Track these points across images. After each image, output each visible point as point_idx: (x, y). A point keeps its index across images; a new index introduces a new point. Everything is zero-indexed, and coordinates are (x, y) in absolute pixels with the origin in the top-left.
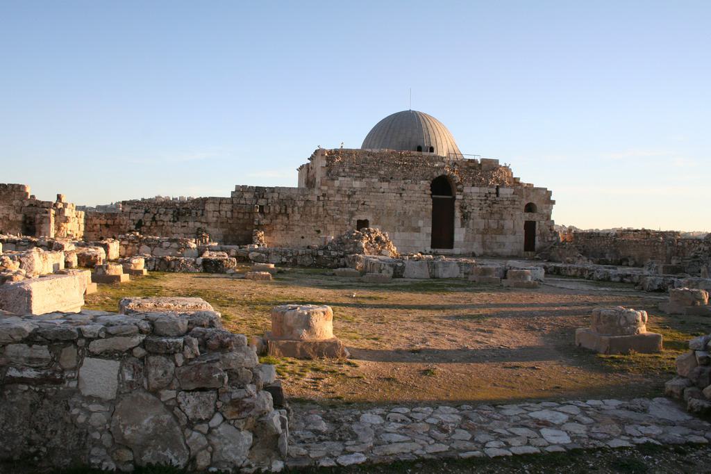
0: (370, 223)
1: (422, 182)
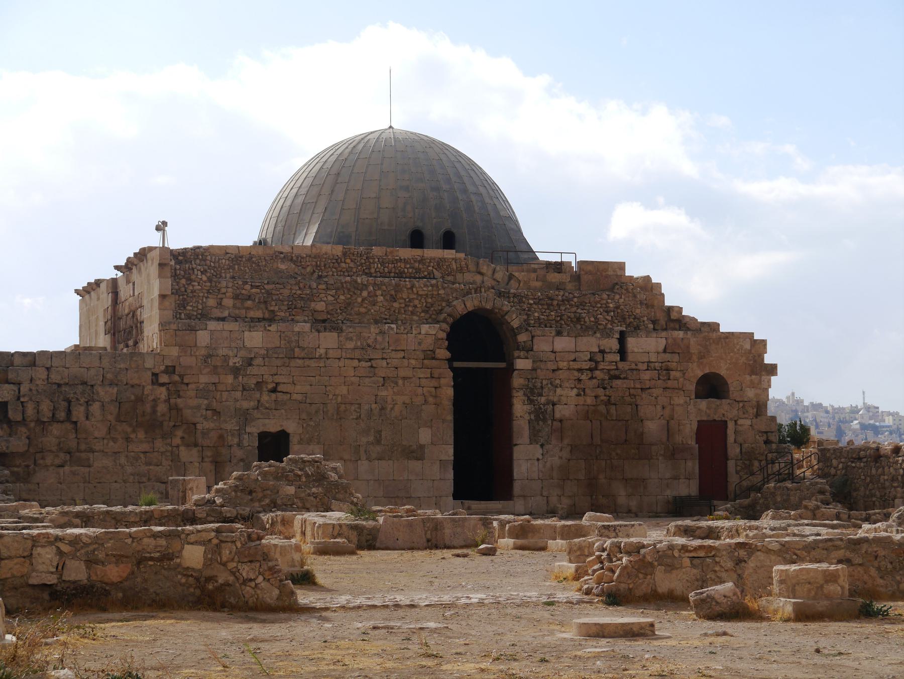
0: (294, 440)
1: (425, 328)
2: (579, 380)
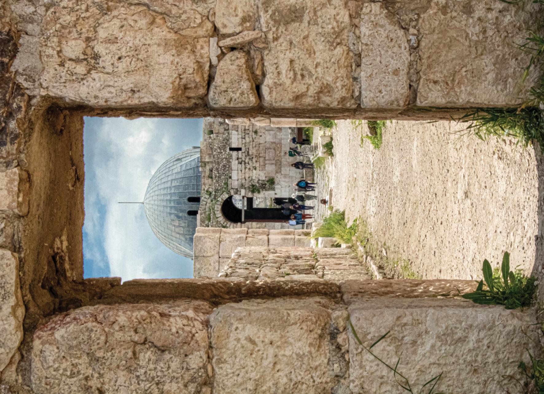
2: (249, 169)
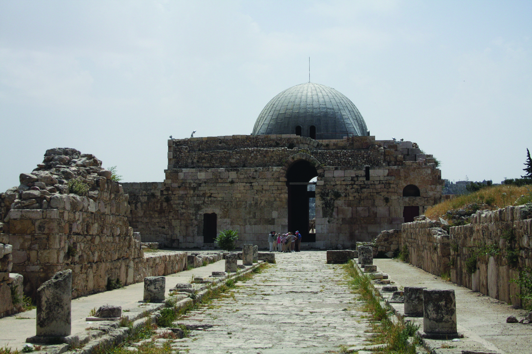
1: (275, 168)
